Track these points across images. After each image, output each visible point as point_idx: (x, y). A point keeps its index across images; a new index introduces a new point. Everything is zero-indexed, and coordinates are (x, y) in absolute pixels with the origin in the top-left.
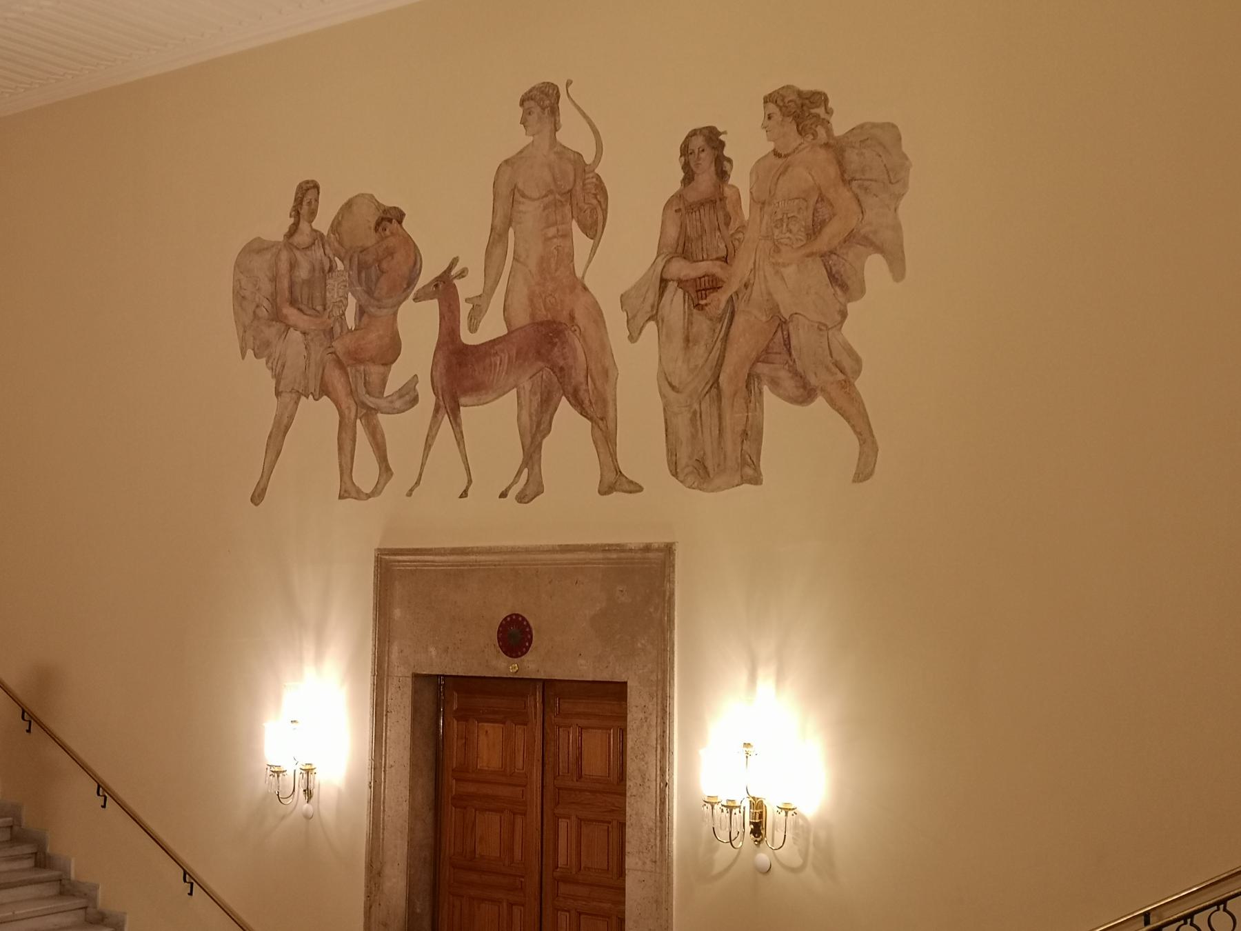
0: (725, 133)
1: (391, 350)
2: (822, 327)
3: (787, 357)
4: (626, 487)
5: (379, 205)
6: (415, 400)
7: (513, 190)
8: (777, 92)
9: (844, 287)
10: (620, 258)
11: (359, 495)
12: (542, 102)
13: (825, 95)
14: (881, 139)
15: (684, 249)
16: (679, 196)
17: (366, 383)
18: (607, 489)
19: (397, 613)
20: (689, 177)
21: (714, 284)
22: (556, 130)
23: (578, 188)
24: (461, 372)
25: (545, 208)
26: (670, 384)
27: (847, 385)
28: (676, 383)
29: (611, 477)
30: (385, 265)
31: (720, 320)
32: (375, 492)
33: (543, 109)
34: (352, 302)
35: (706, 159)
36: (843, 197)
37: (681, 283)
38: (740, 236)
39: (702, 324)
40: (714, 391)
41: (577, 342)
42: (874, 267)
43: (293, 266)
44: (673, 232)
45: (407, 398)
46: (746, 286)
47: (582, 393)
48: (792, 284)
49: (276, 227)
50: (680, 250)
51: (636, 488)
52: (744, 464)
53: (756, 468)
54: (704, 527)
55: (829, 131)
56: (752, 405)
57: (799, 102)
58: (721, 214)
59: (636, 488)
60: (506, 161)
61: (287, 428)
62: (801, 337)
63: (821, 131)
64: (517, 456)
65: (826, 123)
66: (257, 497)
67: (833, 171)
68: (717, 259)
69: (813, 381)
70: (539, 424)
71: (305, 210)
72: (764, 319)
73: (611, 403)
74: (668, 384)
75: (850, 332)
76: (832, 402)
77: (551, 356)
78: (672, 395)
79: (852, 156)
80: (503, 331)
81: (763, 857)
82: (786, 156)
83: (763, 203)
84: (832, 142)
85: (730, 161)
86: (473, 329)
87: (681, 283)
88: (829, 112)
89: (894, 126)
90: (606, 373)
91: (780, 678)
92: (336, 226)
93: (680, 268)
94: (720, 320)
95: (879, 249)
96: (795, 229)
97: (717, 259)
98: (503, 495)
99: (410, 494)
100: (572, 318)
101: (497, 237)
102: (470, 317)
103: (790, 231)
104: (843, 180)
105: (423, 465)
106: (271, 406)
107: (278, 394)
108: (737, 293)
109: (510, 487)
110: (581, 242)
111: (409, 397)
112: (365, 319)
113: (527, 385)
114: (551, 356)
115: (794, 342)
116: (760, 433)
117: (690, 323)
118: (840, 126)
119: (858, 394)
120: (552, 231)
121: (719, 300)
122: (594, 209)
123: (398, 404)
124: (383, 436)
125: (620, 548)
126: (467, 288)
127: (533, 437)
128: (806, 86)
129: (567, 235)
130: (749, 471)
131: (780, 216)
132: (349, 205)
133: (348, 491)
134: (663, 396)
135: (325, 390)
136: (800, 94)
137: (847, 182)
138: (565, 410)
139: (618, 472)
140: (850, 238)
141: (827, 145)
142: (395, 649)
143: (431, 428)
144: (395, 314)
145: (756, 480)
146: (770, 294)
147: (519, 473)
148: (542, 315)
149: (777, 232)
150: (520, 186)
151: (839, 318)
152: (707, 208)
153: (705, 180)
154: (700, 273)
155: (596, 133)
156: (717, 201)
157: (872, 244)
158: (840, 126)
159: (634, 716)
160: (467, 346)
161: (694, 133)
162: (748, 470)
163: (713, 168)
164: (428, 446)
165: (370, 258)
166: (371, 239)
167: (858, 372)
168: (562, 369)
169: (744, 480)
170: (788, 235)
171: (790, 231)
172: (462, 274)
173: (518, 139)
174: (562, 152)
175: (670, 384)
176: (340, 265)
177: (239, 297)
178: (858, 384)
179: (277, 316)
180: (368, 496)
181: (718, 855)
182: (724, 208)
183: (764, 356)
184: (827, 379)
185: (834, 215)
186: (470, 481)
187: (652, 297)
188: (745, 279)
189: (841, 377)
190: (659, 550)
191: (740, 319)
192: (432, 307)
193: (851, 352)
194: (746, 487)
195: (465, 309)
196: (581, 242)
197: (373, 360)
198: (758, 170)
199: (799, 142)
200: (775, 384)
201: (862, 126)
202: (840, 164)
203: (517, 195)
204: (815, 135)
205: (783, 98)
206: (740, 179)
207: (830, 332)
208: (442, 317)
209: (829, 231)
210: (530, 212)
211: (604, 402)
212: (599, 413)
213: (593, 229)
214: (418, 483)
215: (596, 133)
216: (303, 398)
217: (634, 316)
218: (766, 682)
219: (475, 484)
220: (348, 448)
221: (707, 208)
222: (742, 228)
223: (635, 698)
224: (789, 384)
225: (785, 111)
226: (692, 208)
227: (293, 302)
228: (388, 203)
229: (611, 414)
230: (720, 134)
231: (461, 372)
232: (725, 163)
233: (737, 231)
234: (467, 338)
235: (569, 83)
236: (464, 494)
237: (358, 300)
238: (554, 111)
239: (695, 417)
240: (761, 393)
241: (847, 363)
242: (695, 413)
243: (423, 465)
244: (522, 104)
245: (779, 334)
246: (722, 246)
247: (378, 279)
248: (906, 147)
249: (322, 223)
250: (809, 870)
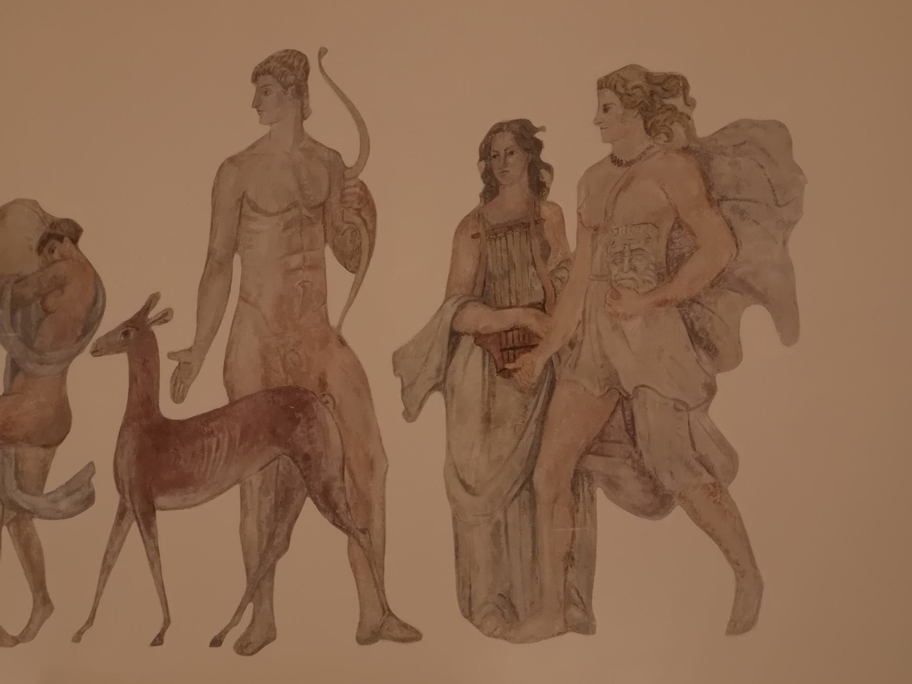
0: (543, 129)
1: (57, 426)
2: (679, 406)
3: (630, 448)
4: (397, 633)
5: (44, 216)
6: (89, 500)
7: (241, 200)
8: (616, 73)
9: (711, 350)
10: (393, 299)
12: (284, 78)
13: (684, 79)
14: (763, 141)
15: (483, 290)
16: (477, 216)
17: (18, 474)
18: (368, 636)
20: (491, 190)
21: (526, 342)
22: (303, 118)
23: (335, 199)
24: (160, 460)
25: (287, 227)
26: (462, 482)
27: (717, 490)
28: (470, 481)
29: (375, 616)
30: (51, 302)
31: (535, 392)
33: (286, 87)
35: (516, 166)
36: (708, 224)
37: (479, 338)
38: (562, 274)
39: (508, 397)
40: (525, 494)
41: (329, 417)
42: (755, 324)
44: (468, 266)
45: (78, 496)
46: (572, 345)
47: (335, 494)
48: (639, 345)
50: (478, 291)
51: (410, 635)
52: (568, 602)
53: (586, 609)
55: (690, 131)
56: (579, 516)
57: (647, 89)
58: (536, 243)
59: (410, 635)
60: (232, 160)
62: (650, 418)
63: (679, 130)
64: (239, 585)
67: (695, 186)
68: (531, 306)
69: (667, 483)
70: (271, 537)
72: (597, 392)
73: (377, 508)
74: (460, 482)
75: (722, 414)
76: (695, 515)
77: (291, 437)
79: (722, 167)
80: (220, 399)
82: (630, 163)
83: (596, 229)
84: (694, 145)
85: (549, 168)
86: (178, 397)
87: (479, 338)
88: (690, 103)
89: (781, 126)
90: (371, 465)
93: (479, 318)
94: (535, 392)
95: (761, 298)
96: (640, 265)
97: (531, 306)
98: (216, 642)
99: (78, 638)
100: (323, 384)
101: (217, 266)
103: (635, 269)
104: (709, 200)
105: (98, 595)
108: (558, 354)
109: (225, 632)
110: (337, 277)
111: (81, 495)
112: (20, 379)
113: (256, 480)
114: (291, 437)
115: (640, 427)
116: (591, 557)
117: (492, 395)
118: (706, 122)
119: (733, 503)
121: (533, 364)
122: (356, 231)
123: (63, 505)
124: (40, 552)
126: (171, 338)
127: (263, 557)
128: (658, 65)
129: (318, 266)
130: (576, 613)
131: (619, 248)
134: (452, 499)
136: (648, 77)
139: (386, 610)
140: (721, 281)
141: (686, 150)
143: (111, 541)
144: (64, 373)
145: (586, 627)
146: (605, 357)
148: (280, 379)
149: (615, 270)
150: (251, 194)
151: (704, 394)
152: (517, 234)
153: (514, 197)
154: (506, 325)
155: (360, 123)
156: (531, 224)
157: (751, 290)
158: (706, 122)
160: (167, 422)
161: (499, 129)
163: (525, 179)
164: (107, 568)
165: (28, 292)
166: (31, 264)
167: (732, 472)
168: (307, 457)
169: (571, 626)
170: (631, 274)
171: (635, 269)
172: (165, 317)
173: (250, 129)
174: (312, 148)
175: (462, 482)
178: (736, 490)
182: (541, 234)
183: (598, 445)
184: (688, 480)
185: (697, 248)
186: (167, 621)
187: (437, 358)
188: (571, 335)
189: (707, 478)
191: (562, 393)
192: (118, 365)
193: (722, 444)
194: (572, 637)
195: (167, 368)
196: (337, 277)
197: (28, 440)
199: (647, 144)
200: (612, 485)
201: (736, 125)
202: (705, 177)
203: (247, 208)
204: (670, 136)
205: (625, 82)
206: (564, 194)
207: (692, 414)
208: (133, 378)
209: (689, 270)
210: (264, 233)
211: (368, 506)
213: (355, 259)
214: (90, 622)
215: (360, 123)
217: (412, 384)
221: (517, 234)
224: (633, 486)
226: (495, 233)
228: (59, 212)
229: (377, 524)
230: (535, 130)
231: (160, 460)
232: (543, 172)
233: (559, 267)
234: (169, 409)
235: (322, 53)
236: (158, 640)
237: (10, 352)
238: (301, 91)
239: (499, 532)
240: (593, 498)
241: (717, 459)
242: (497, 525)
243: (98, 595)
244: (256, 77)
245: (619, 414)
246: (538, 287)
247: (40, 321)
248: (799, 156)
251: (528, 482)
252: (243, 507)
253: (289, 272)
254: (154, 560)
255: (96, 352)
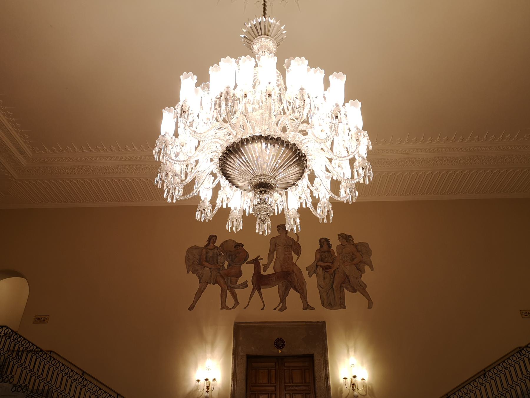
1: (240, 274)
2: (356, 278)
6: (247, 286)
9: (361, 271)
10: (306, 259)
11: (228, 308)
14: (365, 245)
15: (321, 260)
16: (319, 250)
18: (305, 309)
19: (241, 338)
21: (330, 268)
27: (364, 289)
29: (306, 306)
32: (234, 308)
34: (227, 263)
35: (325, 244)
37: (321, 266)
42: (367, 268)
43: (207, 253)
44: (318, 256)
49: (202, 243)
51: (313, 309)
52: (341, 304)
53: (344, 305)
54: (332, 317)
55: (353, 242)
59: (313, 309)
61: (203, 291)
64: (279, 300)
65: (353, 241)
66: (191, 308)
69: (356, 288)
71: (212, 241)
74: (319, 286)
76: (360, 292)
77: (288, 278)
78: (321, 289)
79: (358, 247)
81: (356, 393)
86: (264, 271)
87: (321, 266)
90: (303, 283)
91: (355, 351)
92: (222, 245)
93: (320, 263)
94: (332, 274)
95: (367, 265)
98: (275, 309)
99: (245, 308)
100: (293, 271)
101: (271, 253)
102: (264, 269)
106: (198, 285)
107: (200, 282)
110: (295, 257)
112: (231, 267)
113: (281, 285)
114: (288, 278)
116: (344, 297)
118: (356, 242)
120: (286, 253)
123: (241, 287)
125: (310, 322)
126: (263, 263)
130: (342, 306)
132: (226, 241)
133: (224, 307)
135: (216, 282)
137: (359, 252)
138: (292, 291)
142: (240, 348)
145: (345, 308)
147: (279, 304)
153: (325, 248)
159: (316, 362)
161: (322, 238)
162: (342, 305)
164: (251, 297)
167: (366, 286)
169: (341, 308)
172: (261, 259)
173: (277, 234)
174: (289, 238)
176: (223, 254)
177: (187, 259)
179: (200, 264)
180: (231, 309)
181: (343, 394)
183: (344, 282)
184: (360, 288)
186: (264, 306)
187: (314, 268)
190: (321, 322)
191: (336, 275)
192: (252, 266)
193: (364, 283)
195: (262, 267)
196: (295, 257)
198: (338, 247)
200: (347, 289)
206: (334, 248)
208: (255, 268)
211: (303, 290)
212: (302, 291)
213: (298, 253)
214: (248, 306)
216: (209, 284)
218: (352, 353)
219: (266, 307)
220: (224, 297)
222: (335, 257)
223: (317, 358)
225: (343, 237)
227: (206, 261)
229: (305, 292)
231: (260, 281)
234: (262, 273)
236: (263, 309)
241: (363, 285)
249: (218, 244)
250: (368, 395)
251: (332, 287)
252: (279, 289)
253: (285, 254)
254: (261, 296)
255: (247, 263)
